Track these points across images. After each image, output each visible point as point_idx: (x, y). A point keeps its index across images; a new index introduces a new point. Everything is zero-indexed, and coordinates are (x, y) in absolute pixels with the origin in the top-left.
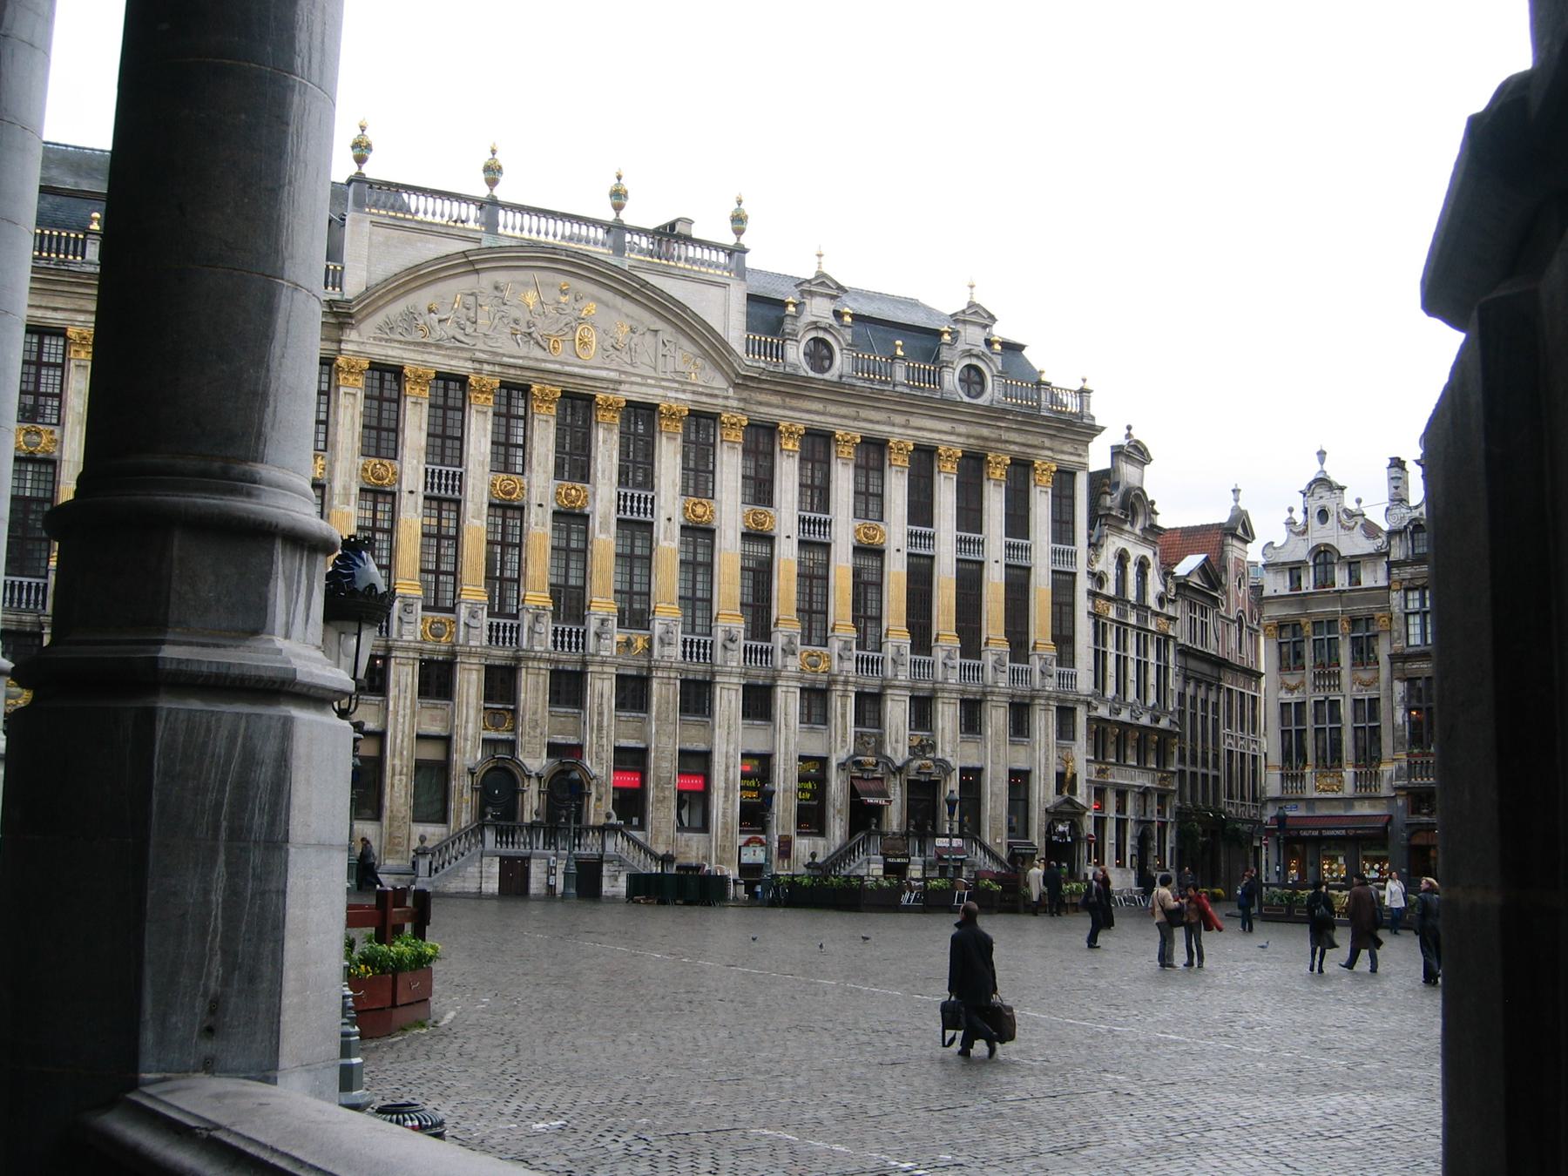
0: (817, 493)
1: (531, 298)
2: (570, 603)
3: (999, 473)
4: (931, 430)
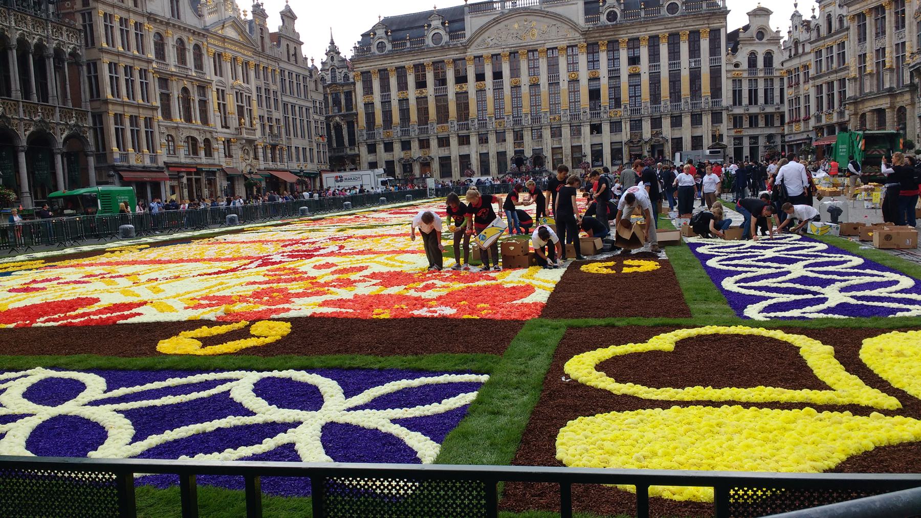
4: (654, 30)
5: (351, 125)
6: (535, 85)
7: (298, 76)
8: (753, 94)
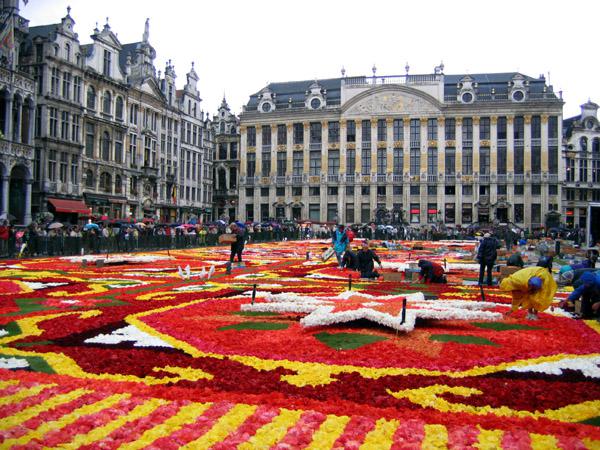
0: (469, 134)
1: (385, 98)
2: (398, 171)
3: (529, 121)
5: (233, 171)
6: (398, 149)
7: (195, 127)
8: (583, 173)
